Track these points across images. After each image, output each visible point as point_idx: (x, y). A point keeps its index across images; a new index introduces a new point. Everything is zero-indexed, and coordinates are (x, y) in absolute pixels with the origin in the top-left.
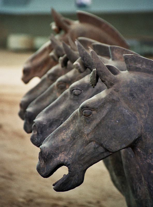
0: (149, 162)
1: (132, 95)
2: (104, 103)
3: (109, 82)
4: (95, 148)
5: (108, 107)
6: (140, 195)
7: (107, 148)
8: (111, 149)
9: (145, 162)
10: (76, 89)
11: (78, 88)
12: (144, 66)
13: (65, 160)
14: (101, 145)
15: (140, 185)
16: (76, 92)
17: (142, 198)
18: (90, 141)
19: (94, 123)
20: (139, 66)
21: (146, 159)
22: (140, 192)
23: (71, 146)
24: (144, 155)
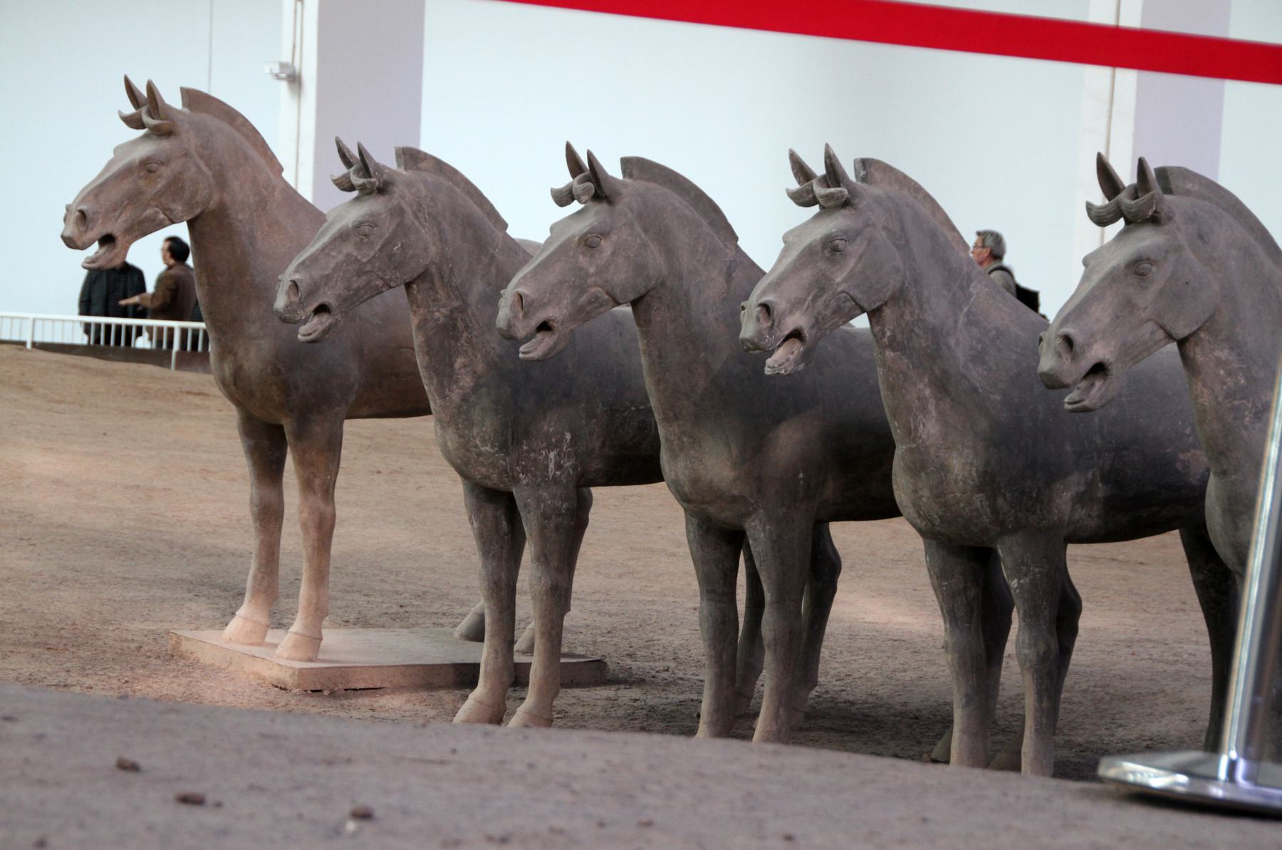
0: (1217, 355)
1: (1201, 237)
2: (1167, 252)
3: (1166, 214)
4: (1153, 333)
5: (1172, 258)
6: (924, 436)
7: (1172, 331)
8: (1176, 334)
9: (1210, 355)
10: (841, 239)
11: (844, 238)
12: (1197, 188)
13: (1104, 355)
14: (1162, 327)
15: (924, 419)
16: (841, 244)
17: (928, 443)
18: (1148, 320)
19: (1154, 288)
20: (1189, 186)
21: (1213, 350)
22: (923, 431)
23: (1112, 329)
24: (1210, 342)
